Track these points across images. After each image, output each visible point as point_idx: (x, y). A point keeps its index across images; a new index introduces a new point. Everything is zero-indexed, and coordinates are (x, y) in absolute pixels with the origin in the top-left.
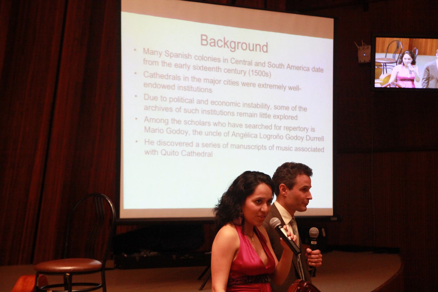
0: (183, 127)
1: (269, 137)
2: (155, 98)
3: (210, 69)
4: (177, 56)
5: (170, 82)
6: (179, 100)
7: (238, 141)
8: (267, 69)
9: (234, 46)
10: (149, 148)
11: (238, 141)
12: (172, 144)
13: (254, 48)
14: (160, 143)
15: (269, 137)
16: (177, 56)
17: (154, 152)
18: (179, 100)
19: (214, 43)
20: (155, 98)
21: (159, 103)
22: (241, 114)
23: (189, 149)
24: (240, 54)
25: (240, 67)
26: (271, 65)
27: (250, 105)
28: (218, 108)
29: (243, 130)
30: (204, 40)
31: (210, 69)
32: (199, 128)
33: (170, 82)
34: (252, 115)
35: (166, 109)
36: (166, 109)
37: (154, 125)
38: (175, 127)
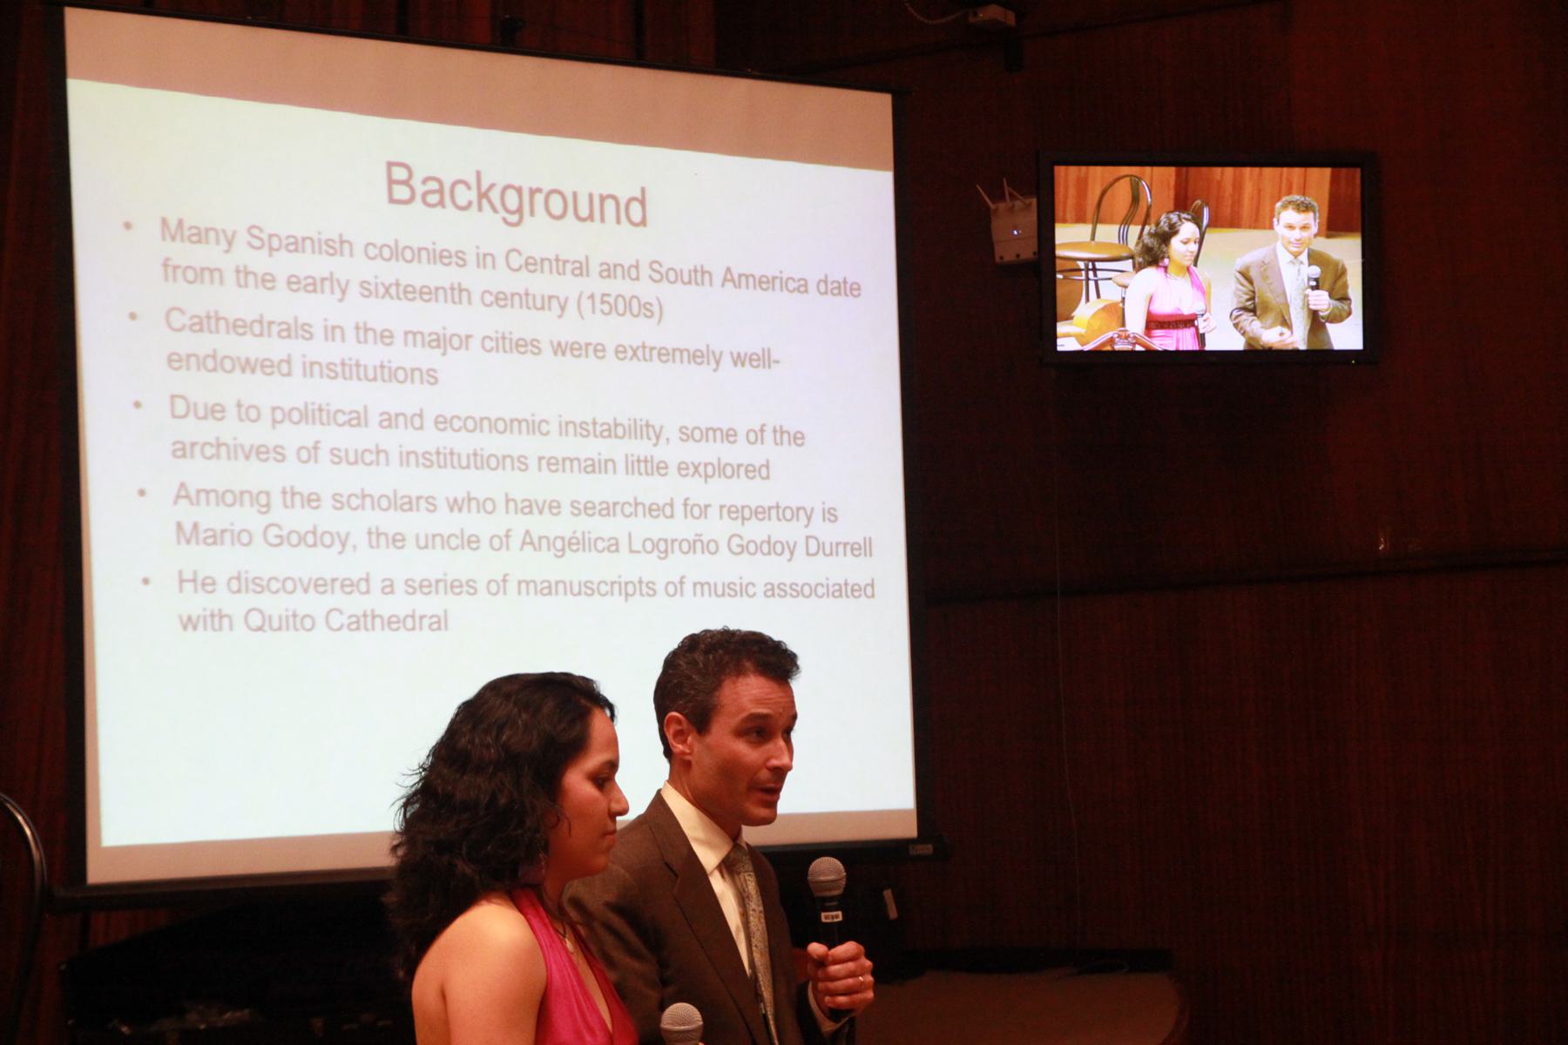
0: (327, 519)
1: (663, 548)
2: (215, 412)
3: (426, 294)
4: (295, 245)
5: (274, 348)
6: (310, 414)
7: (543, 566)
8: (646, 290)
9: (518, 204)
10: (197, 603)
11: (543, 566)
12: (288, 585)
13: (597, 208)
14: (241, 583)
15: (663, 548)
16: (295, 245)
17: (217, 619)
18: (310, 414)
19: (440, 194)
20: (215, 412)
21: (231, 429)
22: (553, 464)
23: (356, 604)
24: (540, 236)
25: (542, 284)
26: (662, 274)
27: (584, 429)
28: (463, 443)
29: (564, 525)
30: (399, 181)
31: (426, 294)
32: (392, 522)
33: (274, 348)
34: (594, 467)
35: (260, 452)
36: (260, 452)
37: (211, 517)
38: (298, 519)
